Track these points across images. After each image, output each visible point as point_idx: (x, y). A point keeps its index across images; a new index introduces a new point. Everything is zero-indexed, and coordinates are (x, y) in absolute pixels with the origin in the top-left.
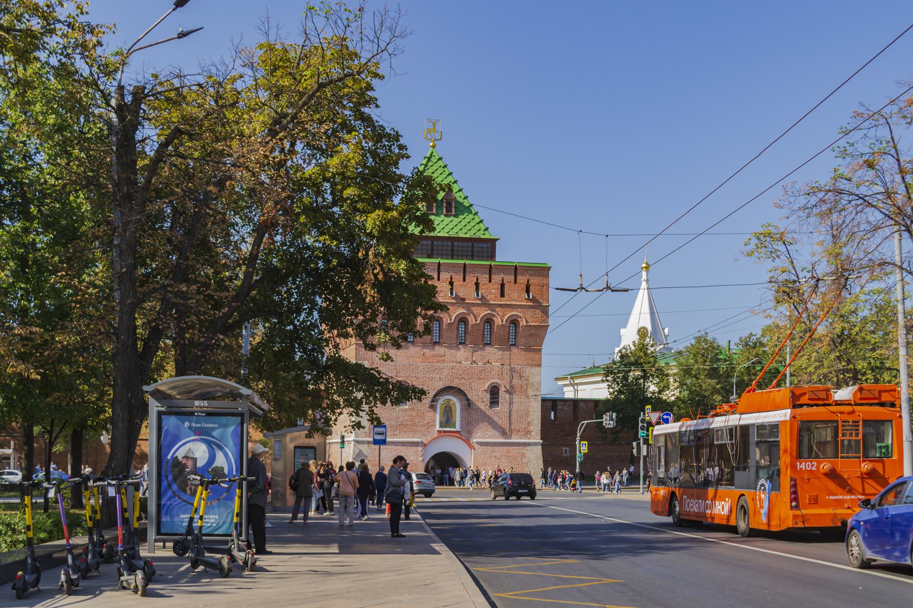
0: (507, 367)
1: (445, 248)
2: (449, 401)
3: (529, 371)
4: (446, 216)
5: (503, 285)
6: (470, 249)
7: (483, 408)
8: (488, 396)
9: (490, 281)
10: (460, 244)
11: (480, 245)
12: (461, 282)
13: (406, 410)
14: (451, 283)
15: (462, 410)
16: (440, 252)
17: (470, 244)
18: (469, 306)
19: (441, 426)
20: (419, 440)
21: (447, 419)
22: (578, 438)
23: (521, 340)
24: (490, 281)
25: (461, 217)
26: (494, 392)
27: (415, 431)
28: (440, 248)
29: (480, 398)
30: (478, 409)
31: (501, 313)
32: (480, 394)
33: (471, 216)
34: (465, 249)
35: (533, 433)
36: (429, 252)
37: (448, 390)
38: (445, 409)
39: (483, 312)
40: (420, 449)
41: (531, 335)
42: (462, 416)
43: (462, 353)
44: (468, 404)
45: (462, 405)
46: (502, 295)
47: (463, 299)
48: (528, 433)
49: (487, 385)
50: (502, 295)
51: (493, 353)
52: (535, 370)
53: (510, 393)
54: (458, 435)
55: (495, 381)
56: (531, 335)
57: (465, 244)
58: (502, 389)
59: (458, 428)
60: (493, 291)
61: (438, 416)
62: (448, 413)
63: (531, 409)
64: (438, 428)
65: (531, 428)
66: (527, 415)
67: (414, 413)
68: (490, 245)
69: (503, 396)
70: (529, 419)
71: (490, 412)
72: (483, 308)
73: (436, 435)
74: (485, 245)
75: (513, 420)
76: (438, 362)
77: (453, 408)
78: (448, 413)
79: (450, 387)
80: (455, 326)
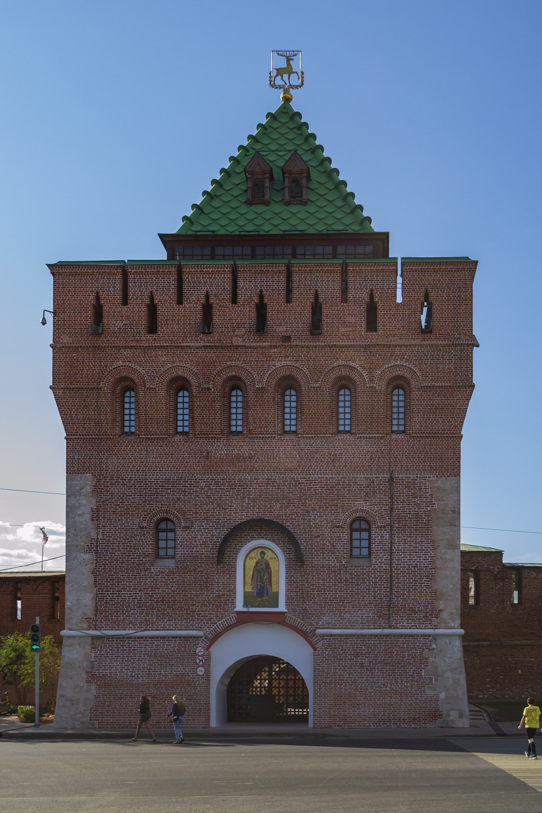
2: (263, 550)
9: (345, 300)
15: (288, 569)
19: (246, 605)
35: (445, 615)
42: (289, 582)
45: (289, 561)
47: (287, 338)
48: (431, 615)
50: (372, 325)
60: (352, 319)
63: (439, 564)
65: (441, 605)
66: (431, 578)
78: (262, 573)
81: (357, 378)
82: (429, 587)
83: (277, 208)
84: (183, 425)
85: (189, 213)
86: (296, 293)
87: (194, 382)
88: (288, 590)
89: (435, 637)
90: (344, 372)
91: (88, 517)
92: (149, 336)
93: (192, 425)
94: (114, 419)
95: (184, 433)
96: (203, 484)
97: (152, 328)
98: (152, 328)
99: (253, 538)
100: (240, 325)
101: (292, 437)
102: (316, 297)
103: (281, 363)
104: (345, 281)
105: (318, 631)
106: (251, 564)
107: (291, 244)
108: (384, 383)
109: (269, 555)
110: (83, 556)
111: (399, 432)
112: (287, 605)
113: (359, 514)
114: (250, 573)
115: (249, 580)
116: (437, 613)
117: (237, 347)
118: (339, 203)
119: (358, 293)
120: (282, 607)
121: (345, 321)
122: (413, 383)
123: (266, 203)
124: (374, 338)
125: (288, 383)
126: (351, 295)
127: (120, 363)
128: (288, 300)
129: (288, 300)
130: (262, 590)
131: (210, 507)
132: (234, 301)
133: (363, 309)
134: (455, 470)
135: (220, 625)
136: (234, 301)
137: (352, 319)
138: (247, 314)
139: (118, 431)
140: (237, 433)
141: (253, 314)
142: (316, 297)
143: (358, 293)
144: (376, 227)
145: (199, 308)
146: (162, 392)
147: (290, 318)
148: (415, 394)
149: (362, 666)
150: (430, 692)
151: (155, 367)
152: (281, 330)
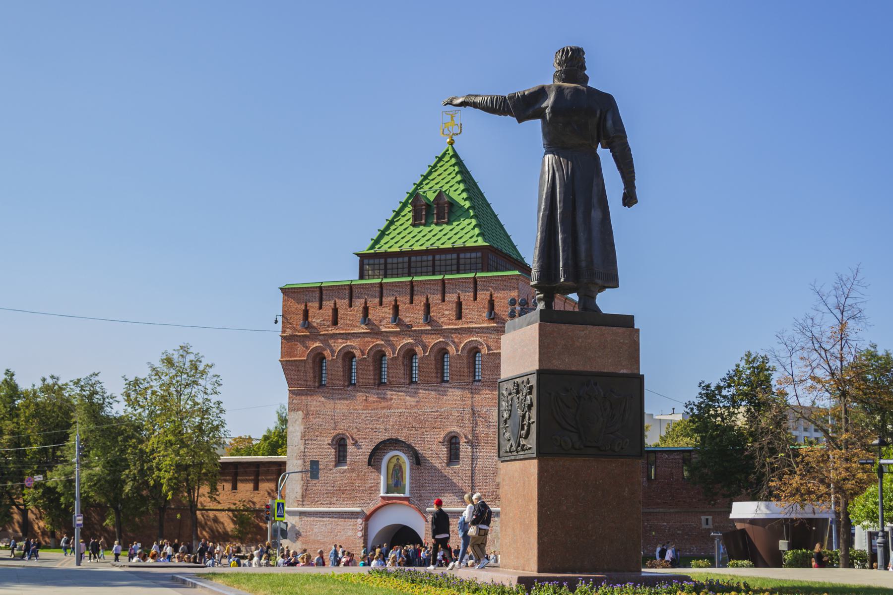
0: (468, 410)
1: (425, 264)
4: (437, 224)
5: (459, 305)
6: (455, 262)
7: (438, 466)
8: (445, 449)
9: (443, 301)
10: (443, 257)
11: (468, 255)
12: (408, 305)
13: (345, 471)
15: (411, 469)
16: (419, 270)
17: (455, 256)
18: (417, 335)
20: (358, 509)
21: (395, 484)
24: (443, 301)
25: (455, 223)
26: (452, 443)
27: (355, 498)
28: (419, 264)
29: (434, 451)
30: (433, 467)
31: (456, 341)
32: (434, 447)
33: (468, 221)
37: (392, 443)
38: (394, 470)
39: (433, 341)
40: (360, 521)
42: (411, 478)
44: (418, 460)
45: (412, 464)
46: (459, 316)
47: (410, 326)
49: (442, 436)
50: (459, 316)
53: (472, 446)
54: (406, 503)
55: (453, 429)
57: (449, 256)
58: (463, 441)
59: (407, 494)
60: (447, 313)
61: (382, 478)
62: (396, 473)
64: (382, 494)
67: (354, 475)
69: (465, 450)
70: (497, 480)
71: (448, 471)
72: (434, 336)
73: (380, 504)
74: (474, 255)
75: (477, 481)
76: (383, 408)
82: (494, 481)
88: (411, 483)
90: (442, 346)
93: (358, 380)
94: (315, 378)
95: (355, 384)
99: (391, 450)
106: (392, 466)
108: (465, 352)
112: (411, 492)
113: (453, 434)
114: (391, 471)
115: (390, 476)
125: (410, 354)
137: (447, 313)
139: (317, 385)
140: (385, 383)
141: (391, 311)
145: (361, 308)
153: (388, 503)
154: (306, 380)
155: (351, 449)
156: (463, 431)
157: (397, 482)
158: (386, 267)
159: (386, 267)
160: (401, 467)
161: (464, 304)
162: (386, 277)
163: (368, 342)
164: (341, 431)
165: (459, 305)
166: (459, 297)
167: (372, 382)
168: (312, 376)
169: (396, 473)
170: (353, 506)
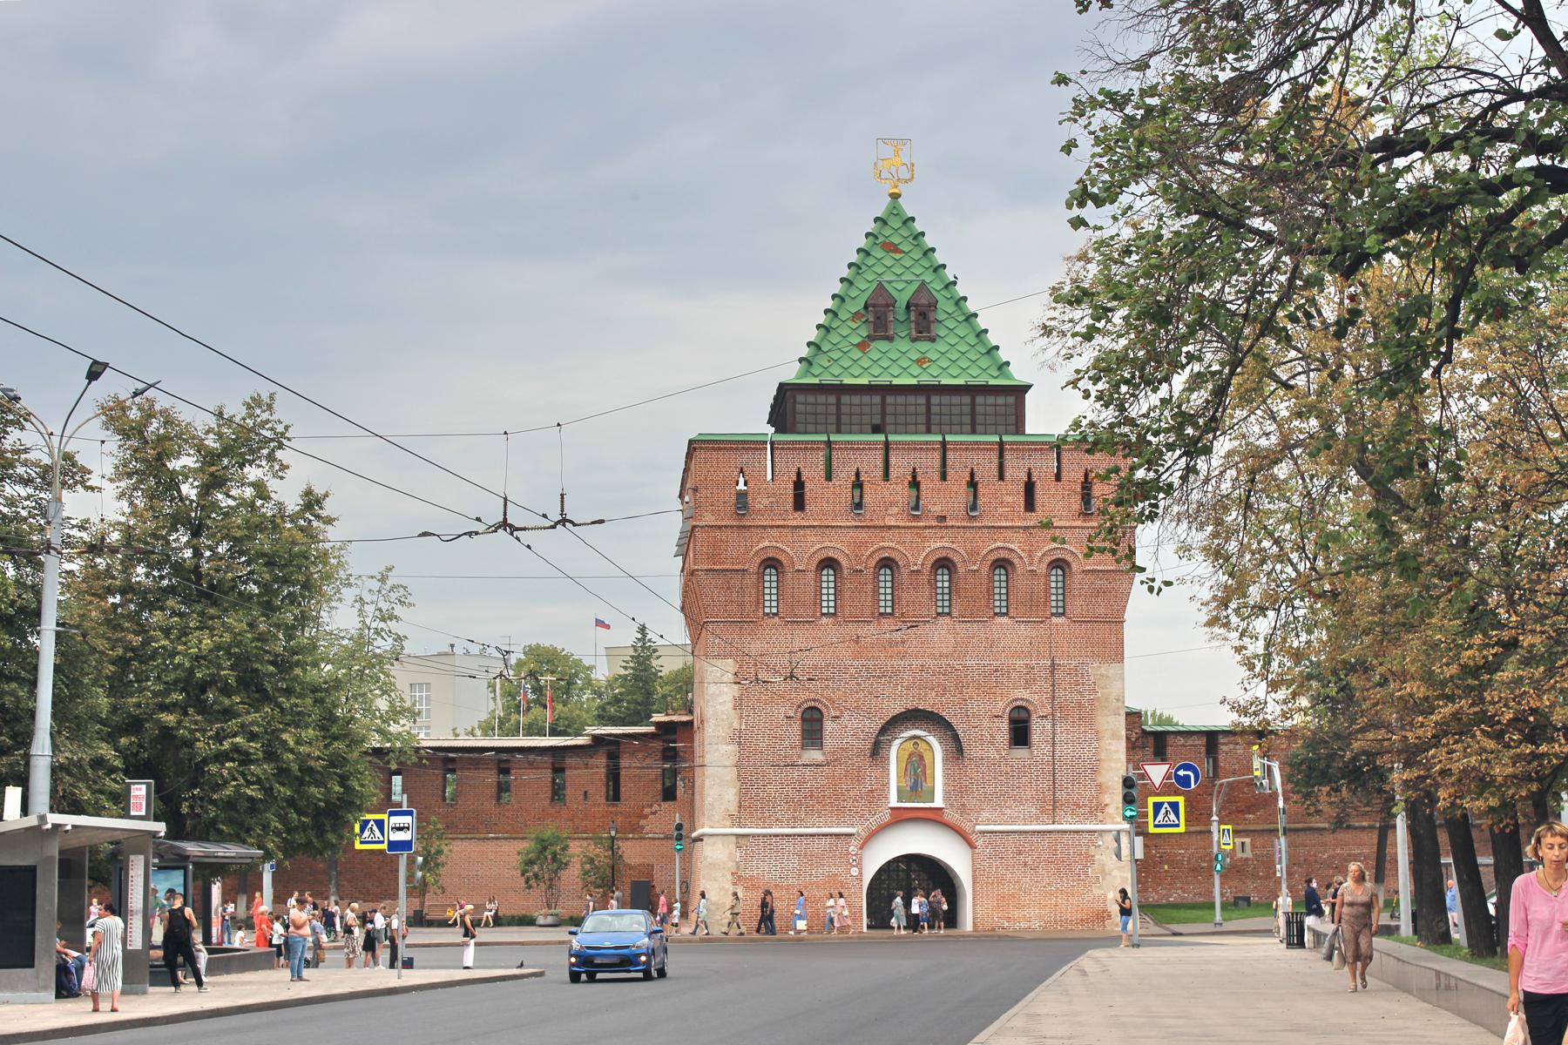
3: (1096, 669)
5: (1030, 487)
9: (1001, 477)
14: (915, 484)
15: (945, 760)
16: (901, 419)
19: (900, 800)
22: (1215, 818)
23: (1077, 606)
24: (1001, 477)
34: (956, 410)
35: (1110, 810)
36: (877, 420)
41: (1097, 593)
42: (946, 776)
43: (941, 634)
45: (945, 751)
46: (1030, 505)
50: (1030, 505)
51: (1011, 635)
52: (1111, 669)
56: (1097, 593)
60: (1010, 499)
62: (917, 769)
63: (1103, 755)
64: (894, 803)
65: (1107, 799)
66: (1095, 770)
67: (839, 771)
68: (1011, 400)
69: (1039, 729)
77: (927, 761)
79: (917, 710)
80: (925, 578)
81: (1016, 561)
83: (904, 345)
84: (828, 605)
85: (805, 352)
86: (951, 472)
87: (844, 562)
89: (1102, 832)
90: (1003, 554)
91: (730, 705)
92: (796, 515)
96: (852, 671)
97: (799, 503)
98: (799, 503)
99: (907, 729)
100: (892, 504)
101: (947, 619)
102: (972, 474)
103: (937, 544)
104: (1001, 456)
105: (978, 828)
107: (930, 405)
109: (922, 746)
110: (725, 747)
111: (1057, 615)
113: (1019, 703)
116: (1101, 808)
117: (890, 527)
118: (972, 340)
119: (1016, 472)
120: (939, 802)
121: (1003, 500)
122: (1074, 566)
123: (890, 339)
124: (1032, 519)
125: (944, 564)
126: (1007, 475)
127: (766, 543)
128: (944, 477)
129: (944, 477)
130: (917, 782)
131: (861, 695)
132: (886, 475)
133: (1021, 488)
134: (1118, 656)
135: (873, 823)
136: (886, 475)
137: (1010, 499)
138: (899, 492)
142: (972, 474)
143: (1016, 472)
144: (1018, 375)
146: (811, 575)
147: (945, 499)
148: (1077, 578)
149: (1025, 864)
150: (1096, 892)
151: (802, 550)
152: (937, 509)
153: (901, 818)
154: (741, 605)
155: (828, 726)
156: (1034, 697)
157: (916, 782)
158: (838, 409)
159: (838, 409)
160: (921, 758)
161: (1038, 485)
162: (838, 431)
163: (864, 544)
164: (812, 696)
165: (1030, 487)
166: (1029, 475)
167: (867, 612)
168: (753, 599)
169: (917, 769)
170: (838, 825)
